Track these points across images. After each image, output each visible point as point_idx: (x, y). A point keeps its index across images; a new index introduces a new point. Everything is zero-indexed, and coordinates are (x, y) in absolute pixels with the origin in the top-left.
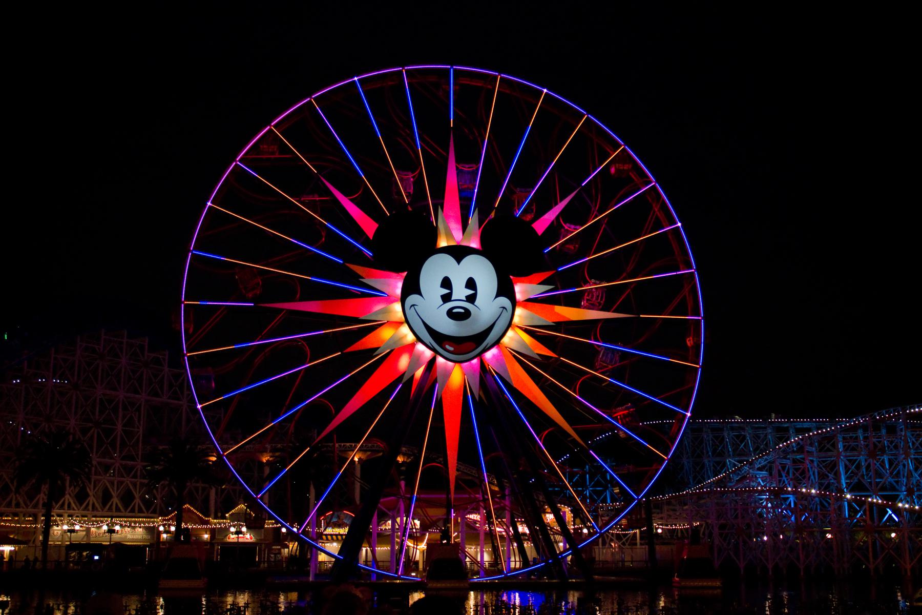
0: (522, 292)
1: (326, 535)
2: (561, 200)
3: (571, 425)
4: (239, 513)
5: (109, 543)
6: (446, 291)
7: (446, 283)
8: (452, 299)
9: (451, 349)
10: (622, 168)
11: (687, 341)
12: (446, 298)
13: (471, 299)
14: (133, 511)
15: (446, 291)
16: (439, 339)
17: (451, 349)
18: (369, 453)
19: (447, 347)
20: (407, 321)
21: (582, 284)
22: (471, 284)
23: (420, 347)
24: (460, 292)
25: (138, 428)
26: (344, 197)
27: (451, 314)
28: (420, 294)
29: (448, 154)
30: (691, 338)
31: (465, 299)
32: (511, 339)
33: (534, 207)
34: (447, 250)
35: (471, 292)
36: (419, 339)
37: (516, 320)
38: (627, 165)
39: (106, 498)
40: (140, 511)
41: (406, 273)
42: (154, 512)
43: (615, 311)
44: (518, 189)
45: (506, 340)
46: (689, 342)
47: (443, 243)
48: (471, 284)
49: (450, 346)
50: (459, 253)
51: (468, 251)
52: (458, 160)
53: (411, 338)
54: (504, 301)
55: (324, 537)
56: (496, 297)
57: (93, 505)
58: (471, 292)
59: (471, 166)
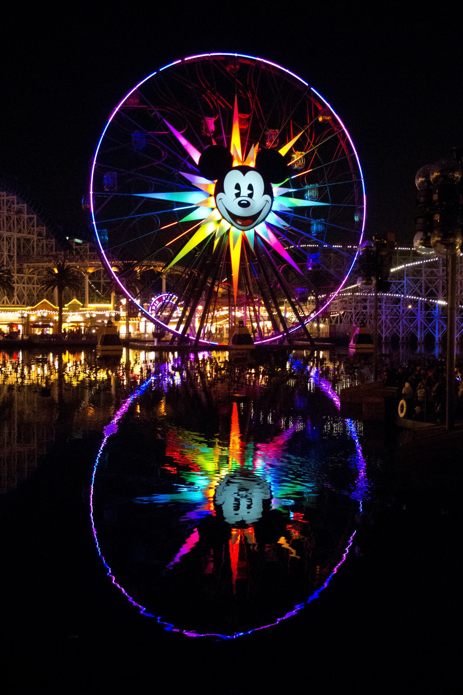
0: (278, 192)
1: (123, 317)
2: (293, 138)
3: (296, 262)
4: (73, 304)
5: (21, 323)
6: (238, 191)
7: (238, 187)
8: (241, 196)
9: (240, 223)
10: (326, 118)
11: (355, 217)
12: (238, 195)
13: (251, 196)
14: (14, 303)
15: (238, 191)
16: (234, 218)
17: (240, 223)
18: (146, 267)
19: (238, 222)
20: (217, 207)
21: (302, 185)
22: (250, 187)
23: (224, 222)
24: (245, 192)
25: (14, 253)
26: (177, 131)
27: (240, 204)
28: (223, 192)
29: (233, 107)
30: (358, 217)
31: (247, 196)
32: (272, 219)
33: (278, 141)
34: (238, 168)
35: (250, 192)
36: (223, 217)
37: (273, 209)
38: (329, 117)
39: (21, 297)
40: (18, 303)
41: (216, 181)
42: (24, 304)
43: (320, 201)
44: (271, 130)
45: (268, 220)
46: (356, 219)
47: (236, 164)
48: (250, 187)
49: (240, 221)
50: (244, 170)
51: (249, 169)
52: (239, 112)
53: (219, 217)
54: (268, 197)
55: (122, 318)
56: (264, 194)
57: (17, 302)
58: (250, 192)
59: (245, 115)
